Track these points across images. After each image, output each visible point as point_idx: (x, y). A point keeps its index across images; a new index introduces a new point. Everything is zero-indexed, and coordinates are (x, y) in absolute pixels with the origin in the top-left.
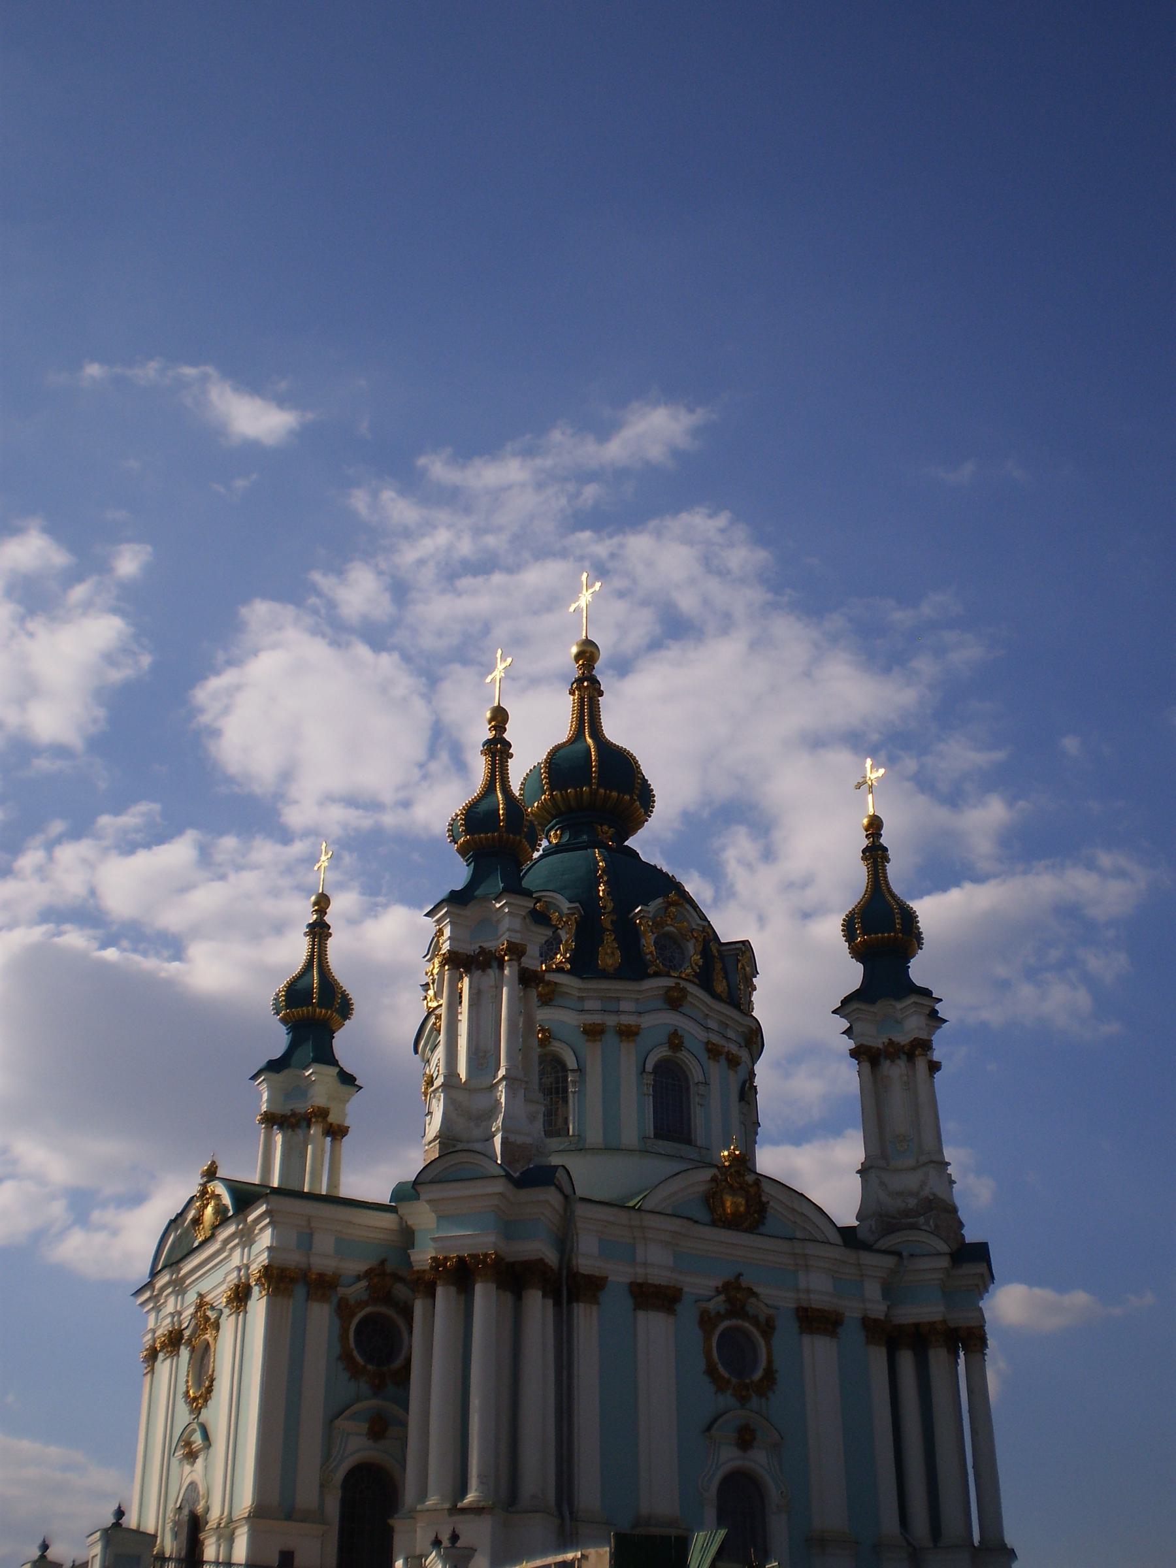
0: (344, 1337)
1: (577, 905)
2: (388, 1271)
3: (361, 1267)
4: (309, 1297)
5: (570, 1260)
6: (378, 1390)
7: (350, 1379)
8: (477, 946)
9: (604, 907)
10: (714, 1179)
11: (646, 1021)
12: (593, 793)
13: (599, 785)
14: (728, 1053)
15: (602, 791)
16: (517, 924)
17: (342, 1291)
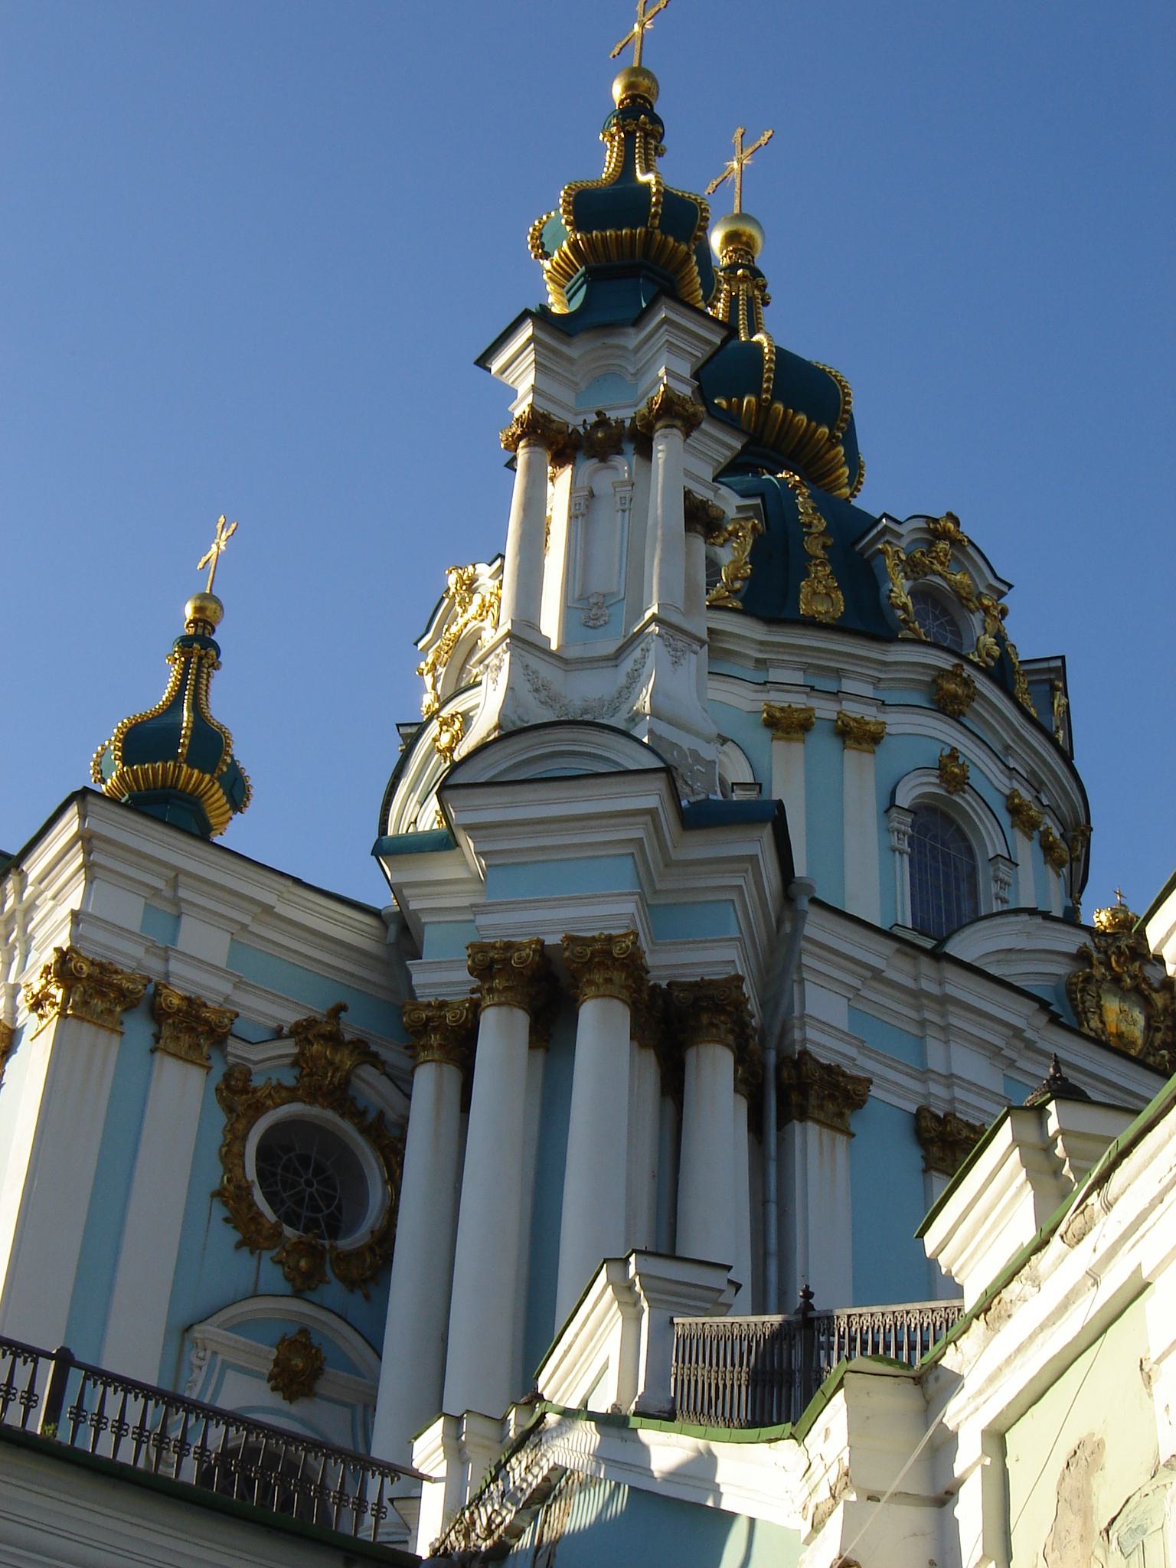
0: (231, 1155)
1: (758, 501)
2: (348, 1037)
3: (290, 1017)
4: (157, 1046)
5: (785, 1030)
6: (303, 1285)
7: (239, 1245)
8: (593, 418)
9: (809, 525)
10: (1082, 957)
11: (896, 722)
12: (764, 409)
13: (776, 396)
14: (1046, 833)
15: (779, 407)
16: (685, 369)
17: (234, 1047)
